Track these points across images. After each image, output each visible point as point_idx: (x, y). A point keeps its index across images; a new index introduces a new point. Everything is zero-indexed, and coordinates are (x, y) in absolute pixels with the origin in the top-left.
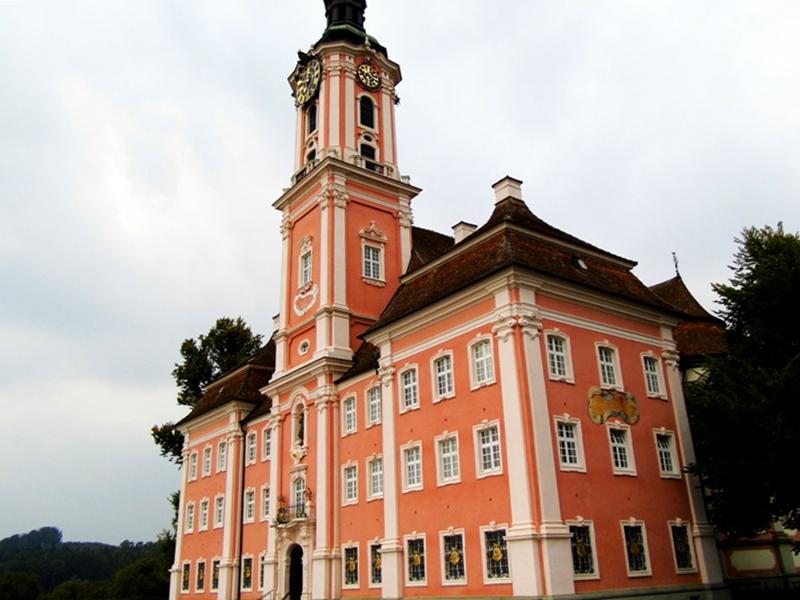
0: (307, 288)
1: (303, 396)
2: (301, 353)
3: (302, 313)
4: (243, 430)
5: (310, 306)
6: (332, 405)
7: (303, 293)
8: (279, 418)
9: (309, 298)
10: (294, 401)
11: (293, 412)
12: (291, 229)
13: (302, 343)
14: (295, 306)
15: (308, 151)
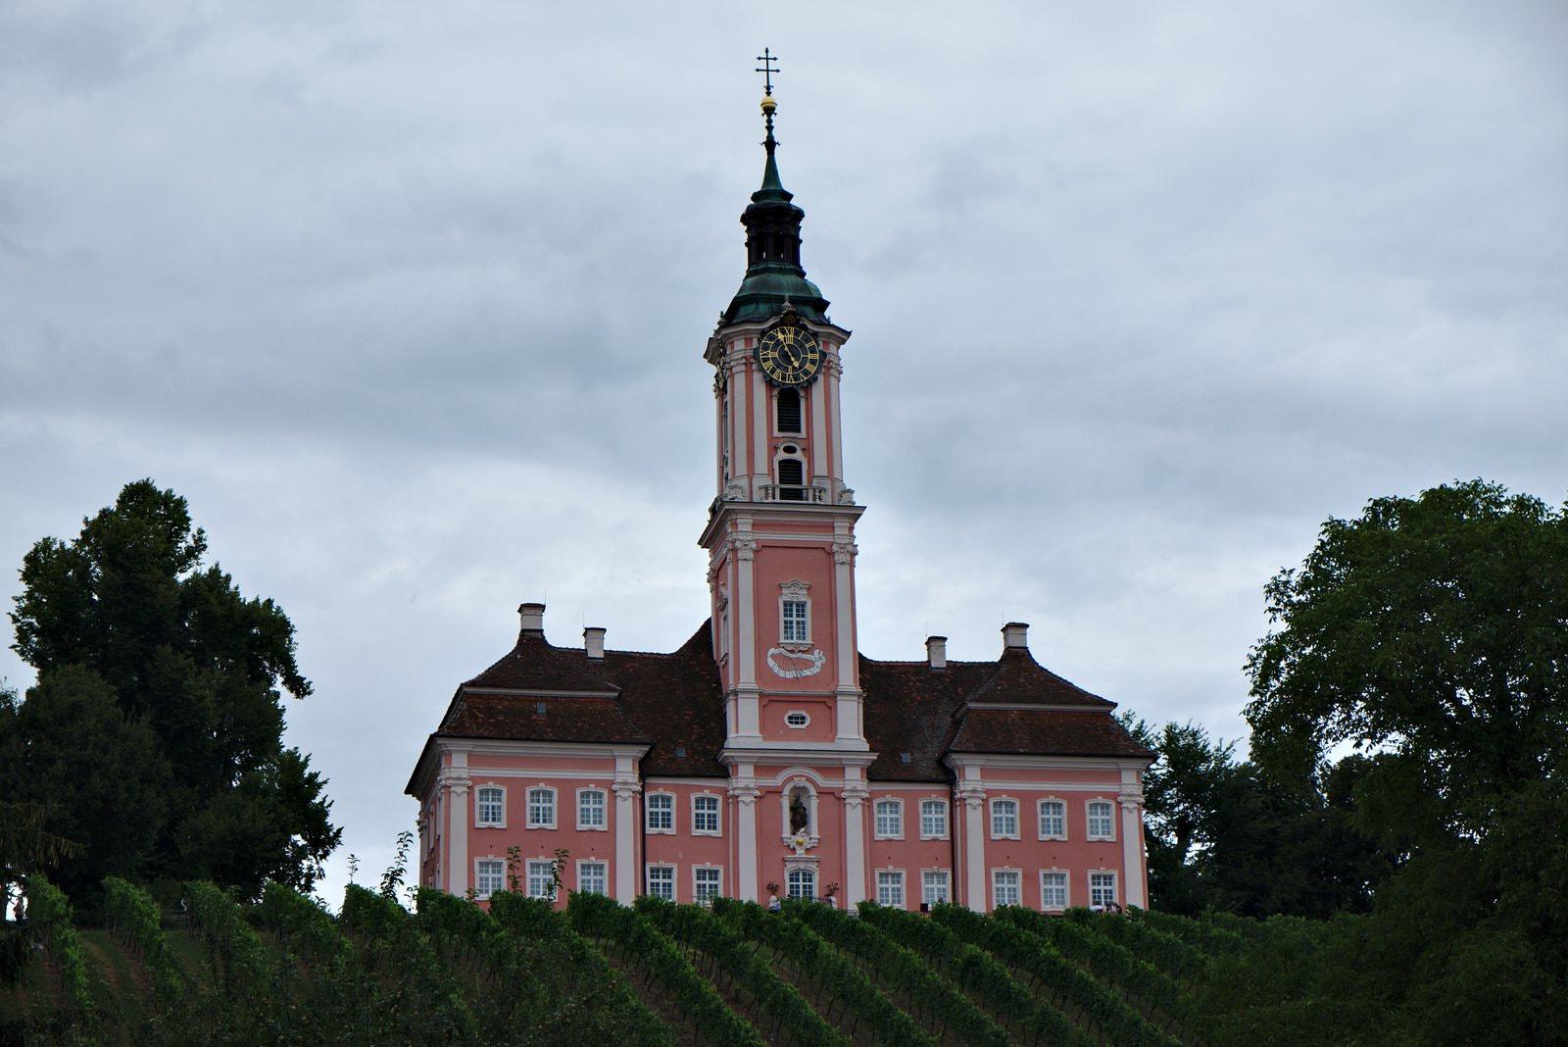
0: (802, 648)
1: (808, 779)
2: (786, 721)
3: (790, 675)
4: (643, 787)
5: (807, 673)
6: (867, 803)
7: (792, 652)
8: (757, 793)
9: (809, 664)
10: (791, 779)
11: (786, 791)
12: (756, 552)
13: (790, 713)
14: (771, 662)
15: (782, 455)
